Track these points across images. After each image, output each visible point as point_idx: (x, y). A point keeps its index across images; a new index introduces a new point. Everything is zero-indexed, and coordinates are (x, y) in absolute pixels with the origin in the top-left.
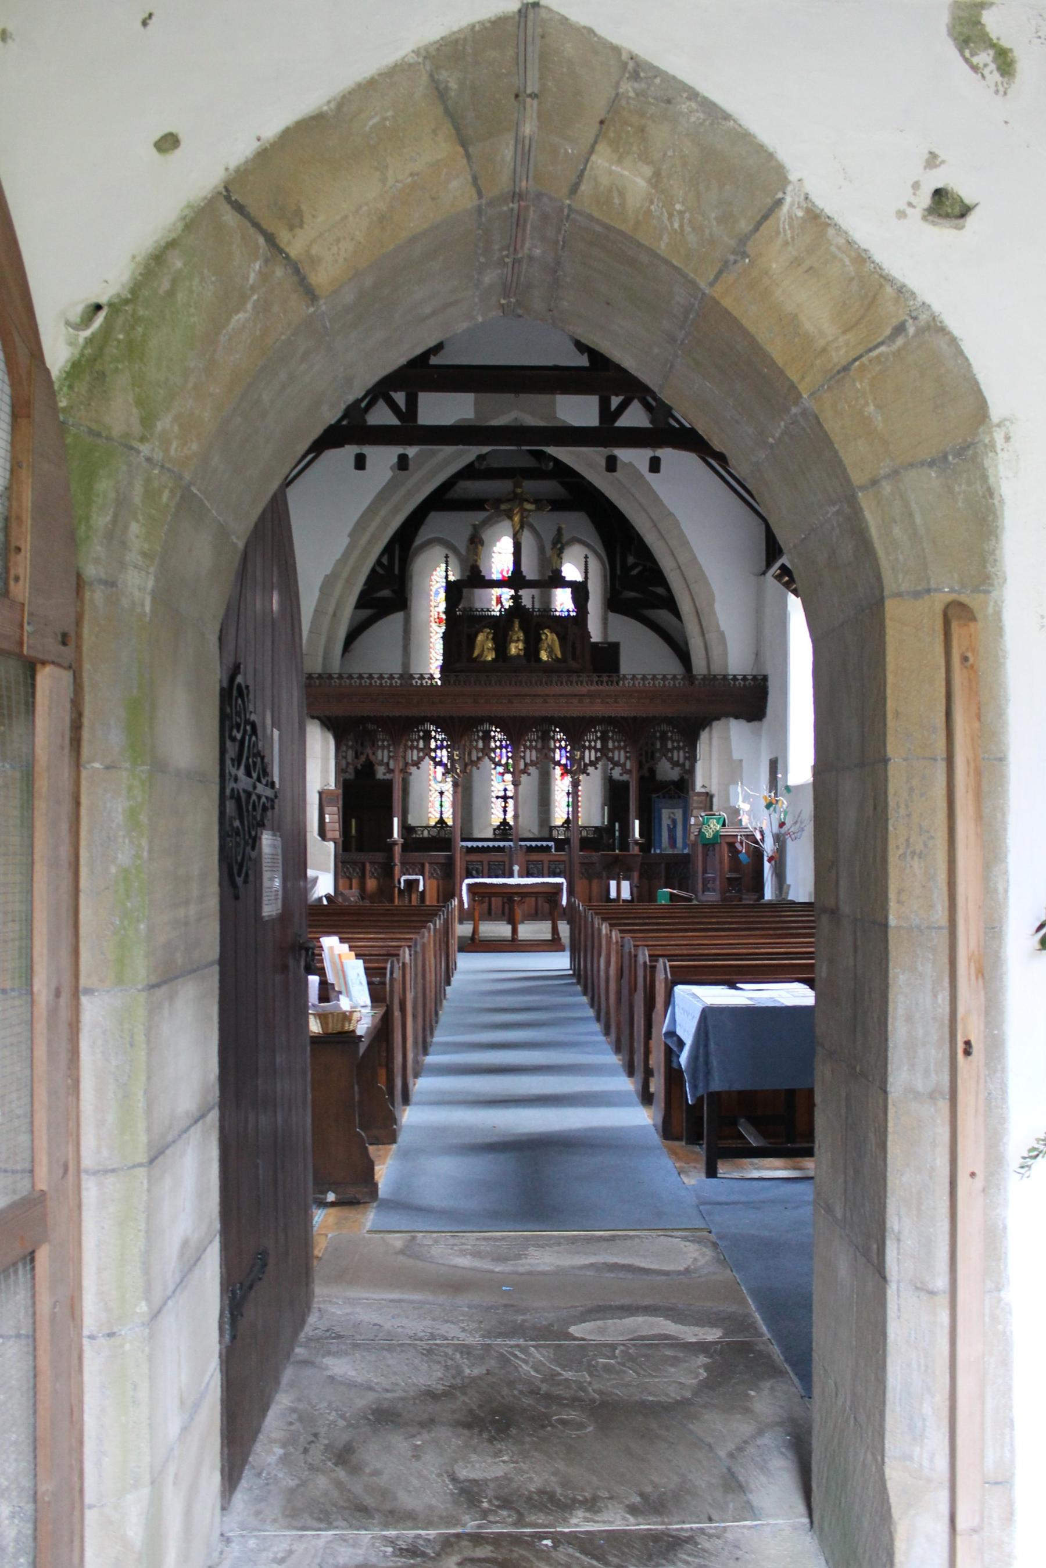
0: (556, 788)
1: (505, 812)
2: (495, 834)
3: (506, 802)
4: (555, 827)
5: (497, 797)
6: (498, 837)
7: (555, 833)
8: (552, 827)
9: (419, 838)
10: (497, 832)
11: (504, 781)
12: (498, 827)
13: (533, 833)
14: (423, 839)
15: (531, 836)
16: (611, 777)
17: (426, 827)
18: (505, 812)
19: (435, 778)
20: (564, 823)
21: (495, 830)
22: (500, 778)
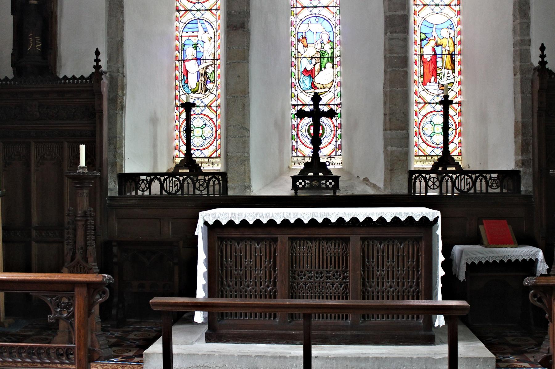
0: (414, 98)
1: (316, 141)
2: (295, 187)
3: (317, 125)
4: (420, 172)
5: (301, 114)
6: (301, 194)
7: (420, 186)
8: (412, 173)
9: (143, 197)
10: (300, 183)
11: (313, 86)
12: (302, 175)
13: (374, 186)
14: (151, 197)
15: (370, 191)
16: (543, 63)
17: (155, 176)
18: (316, 141)
19: (185, 83)
20: (436, 166)
21: (295, 179)
22: (306, 82)
